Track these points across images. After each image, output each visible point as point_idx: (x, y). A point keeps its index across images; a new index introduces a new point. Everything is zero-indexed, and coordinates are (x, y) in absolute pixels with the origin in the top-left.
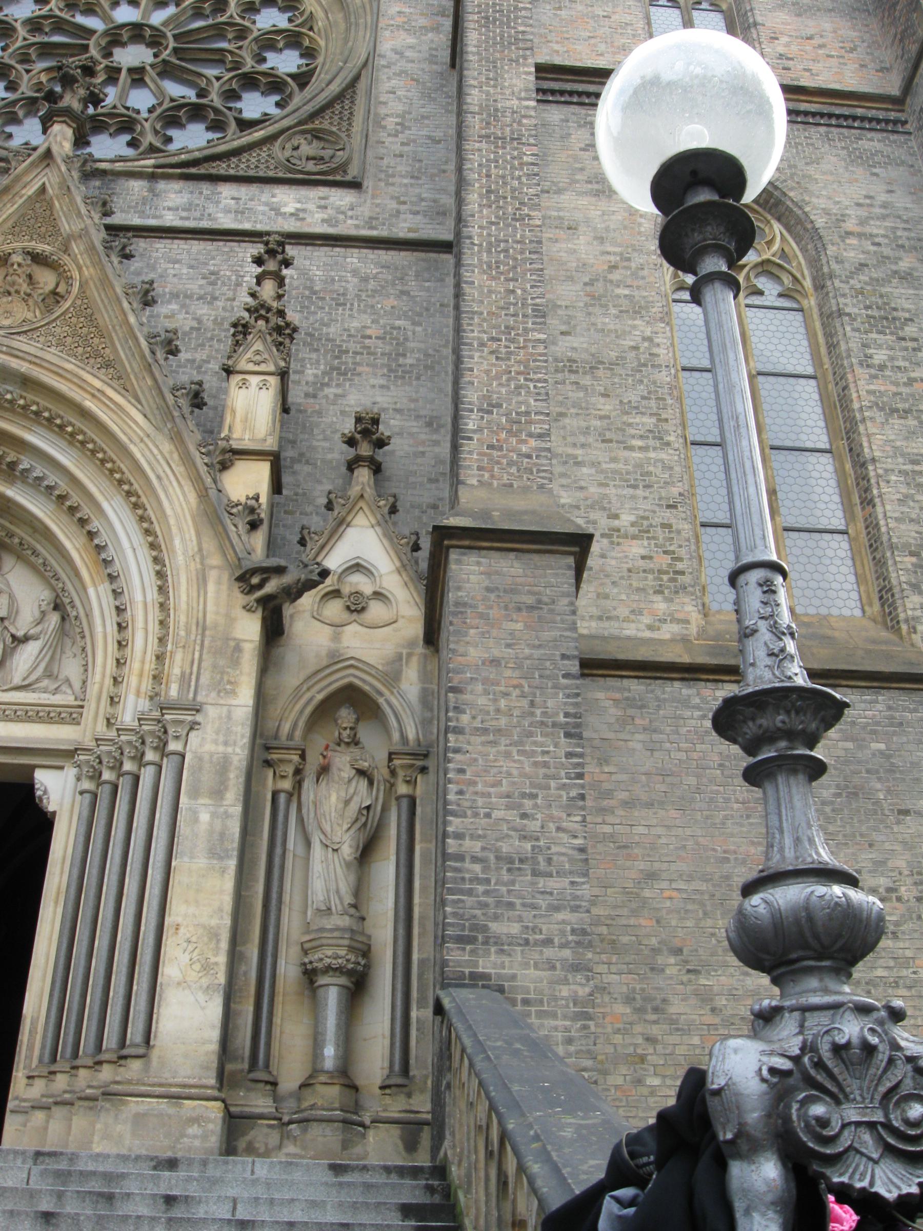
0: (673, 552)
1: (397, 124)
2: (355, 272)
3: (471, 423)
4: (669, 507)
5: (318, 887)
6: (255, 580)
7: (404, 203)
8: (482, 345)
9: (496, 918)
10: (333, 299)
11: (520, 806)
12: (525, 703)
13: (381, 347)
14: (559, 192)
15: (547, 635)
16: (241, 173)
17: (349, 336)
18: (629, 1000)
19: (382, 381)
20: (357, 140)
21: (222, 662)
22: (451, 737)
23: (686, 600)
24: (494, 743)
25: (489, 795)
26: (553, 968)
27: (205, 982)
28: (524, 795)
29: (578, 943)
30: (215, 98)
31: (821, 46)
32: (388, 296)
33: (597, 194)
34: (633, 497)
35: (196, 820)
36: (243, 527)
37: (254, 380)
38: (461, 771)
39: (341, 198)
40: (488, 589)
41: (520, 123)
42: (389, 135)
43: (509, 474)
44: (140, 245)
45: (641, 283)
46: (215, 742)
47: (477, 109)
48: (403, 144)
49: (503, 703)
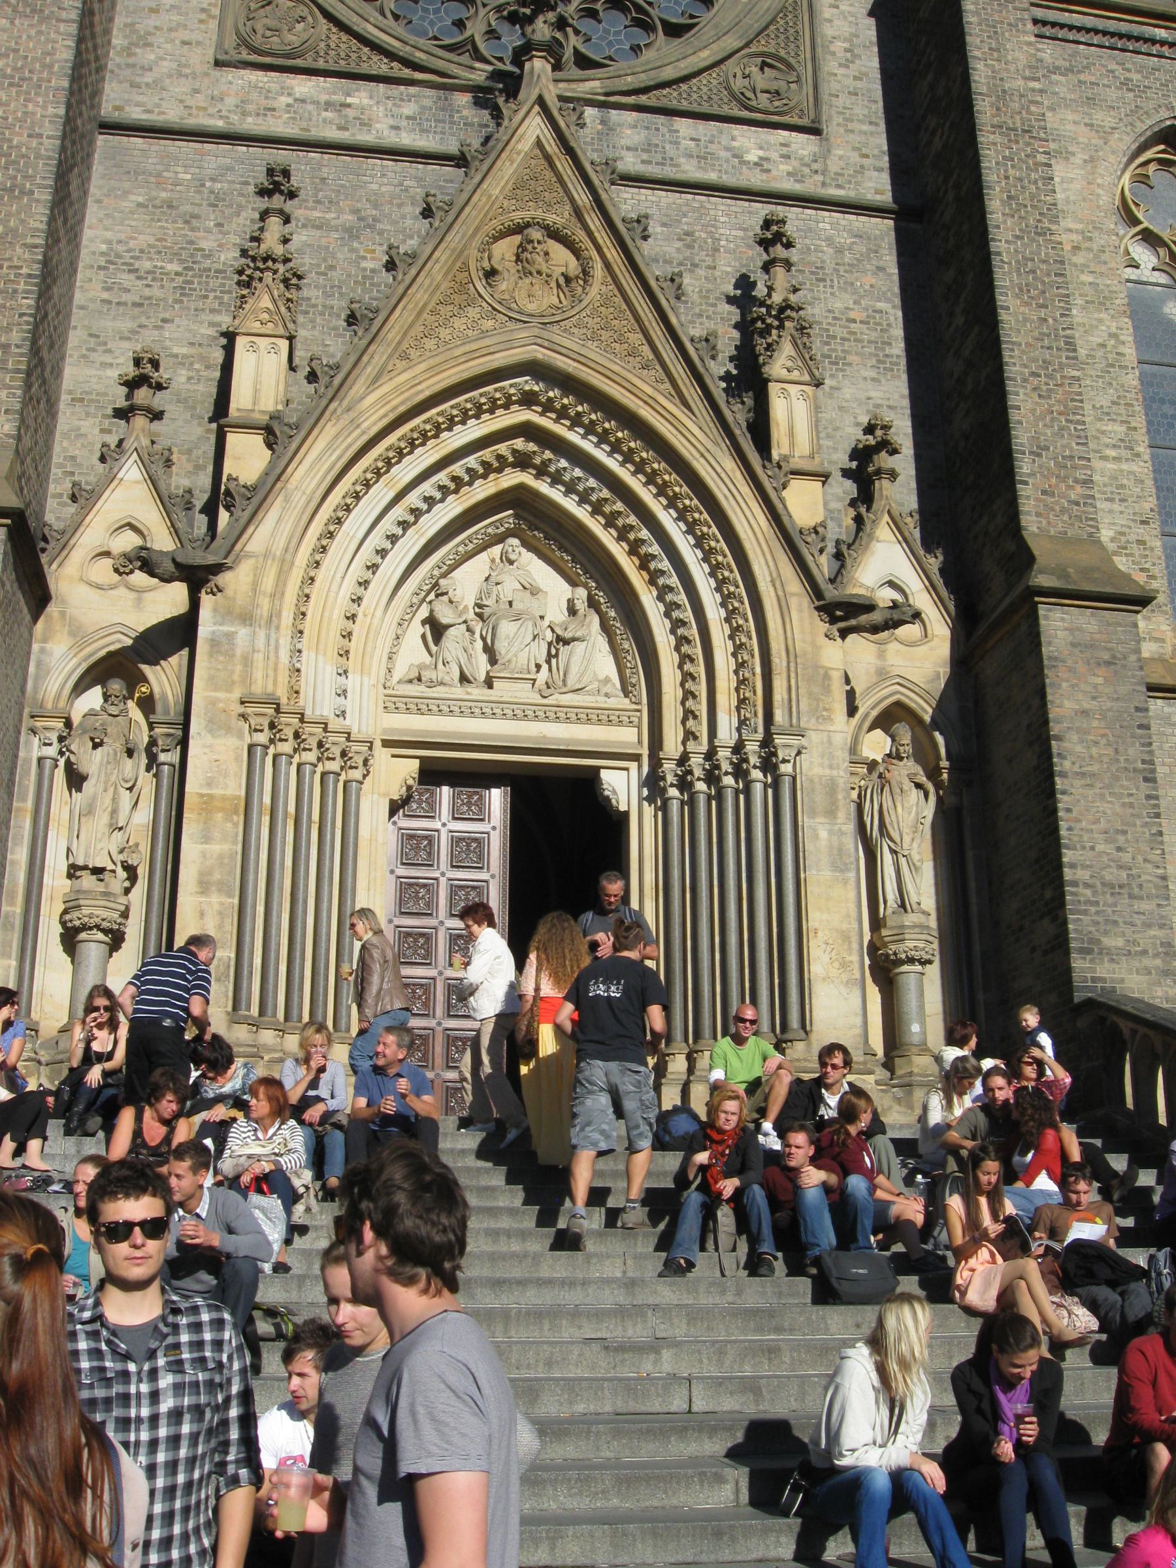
0: (1148, 570)
1: (847, 50)
2: (829, 240)
3: (1024, 466)
4: (1143, 522)
6: (839, 613)
7: (867, 156)
8: (1025, 380)
9: (1106, 933)
10: (812, 273)
11: (1115, 841)
12: (1110, 751)
13: (868, 335)
15: (1123, 689)
16: (695, 108)
17: (835, 318)
21: (816, 690)
22: (1058, 780)
23: (1161, 619)
24: (1091, 786)
25: (1092, 831)
26: (1150, 973)
27: (845, 977)
28: (1117, 832)
29: (1166, 954)
32: (864, 272)
34: (1111, 511)
35: (816, 837)
36: (816, 554)
37: (793, 389)
38: (1069, 810)
39: (802, 144)
40: (1073, 645)
41: (1029, 112)
42: (840, 65)
43: (1064, 522)
45: (1103, 268)
46: (822, 765)
47: (984, 90)
48: (855, 78)
49: (1094, 751)
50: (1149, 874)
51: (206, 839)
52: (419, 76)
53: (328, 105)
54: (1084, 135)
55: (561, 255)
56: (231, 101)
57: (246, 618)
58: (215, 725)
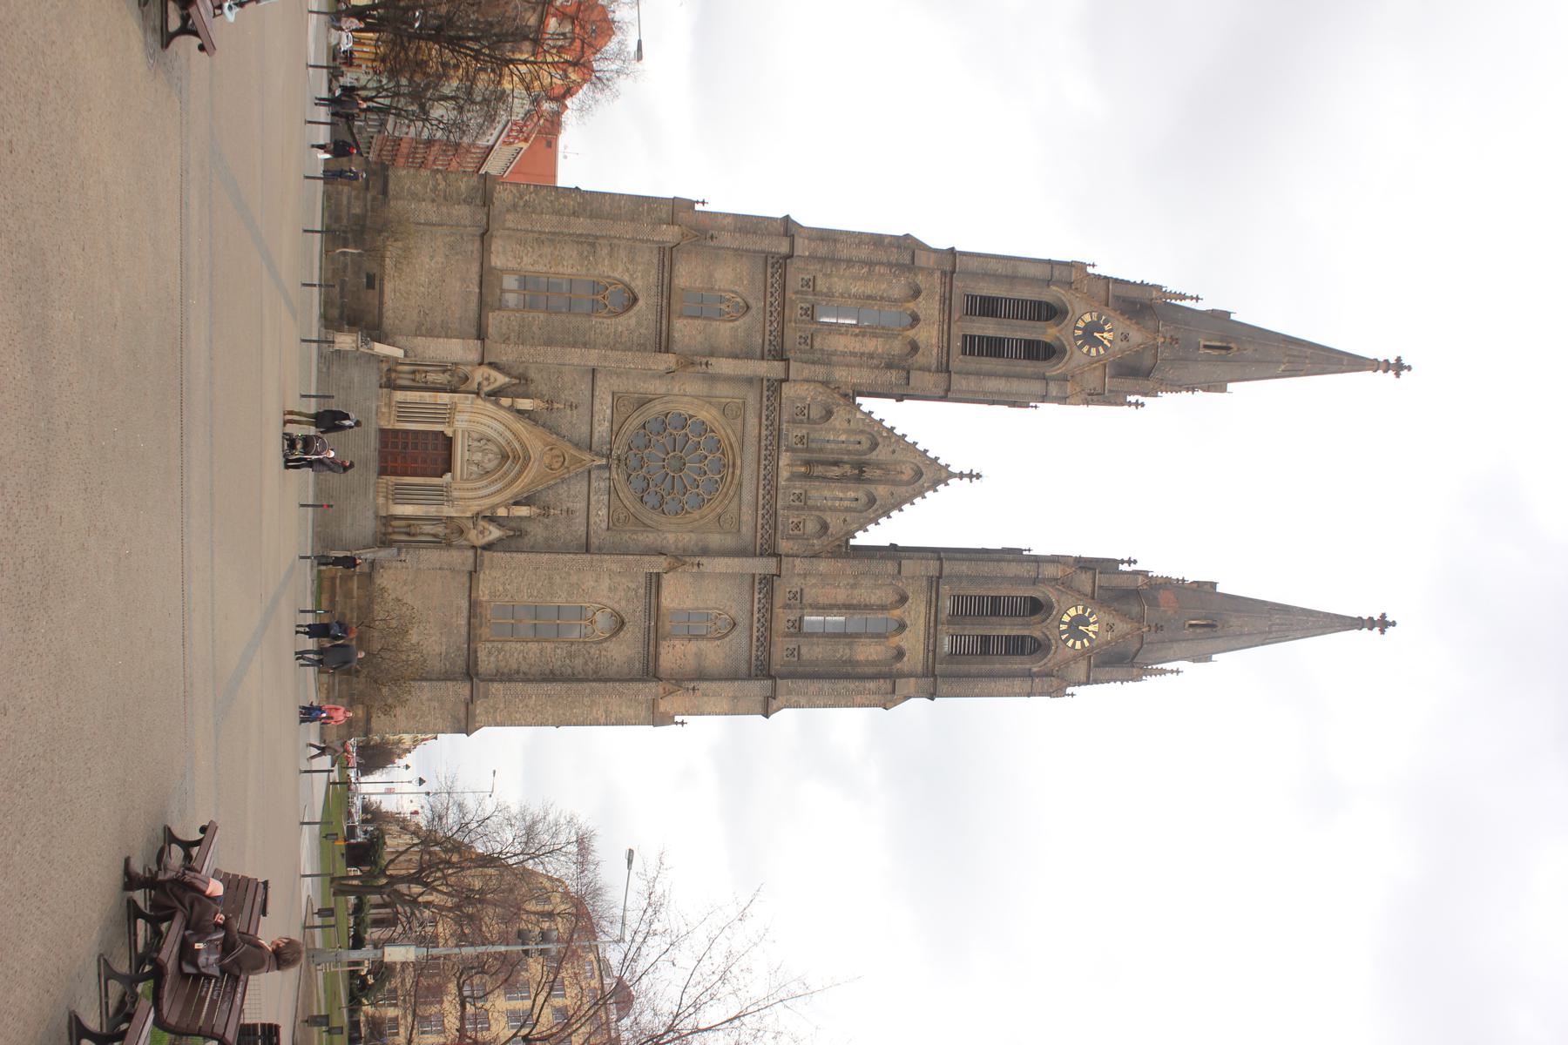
5: (424, 527)
20: (627, 528)
30: (652, 489)
31: (681, 659)
33: (610, 588)
39: (604, 525)
44: (587, 479)
52: (613, 438)
55: (559, 464)
56: (604, 396)
57: (472, 403)
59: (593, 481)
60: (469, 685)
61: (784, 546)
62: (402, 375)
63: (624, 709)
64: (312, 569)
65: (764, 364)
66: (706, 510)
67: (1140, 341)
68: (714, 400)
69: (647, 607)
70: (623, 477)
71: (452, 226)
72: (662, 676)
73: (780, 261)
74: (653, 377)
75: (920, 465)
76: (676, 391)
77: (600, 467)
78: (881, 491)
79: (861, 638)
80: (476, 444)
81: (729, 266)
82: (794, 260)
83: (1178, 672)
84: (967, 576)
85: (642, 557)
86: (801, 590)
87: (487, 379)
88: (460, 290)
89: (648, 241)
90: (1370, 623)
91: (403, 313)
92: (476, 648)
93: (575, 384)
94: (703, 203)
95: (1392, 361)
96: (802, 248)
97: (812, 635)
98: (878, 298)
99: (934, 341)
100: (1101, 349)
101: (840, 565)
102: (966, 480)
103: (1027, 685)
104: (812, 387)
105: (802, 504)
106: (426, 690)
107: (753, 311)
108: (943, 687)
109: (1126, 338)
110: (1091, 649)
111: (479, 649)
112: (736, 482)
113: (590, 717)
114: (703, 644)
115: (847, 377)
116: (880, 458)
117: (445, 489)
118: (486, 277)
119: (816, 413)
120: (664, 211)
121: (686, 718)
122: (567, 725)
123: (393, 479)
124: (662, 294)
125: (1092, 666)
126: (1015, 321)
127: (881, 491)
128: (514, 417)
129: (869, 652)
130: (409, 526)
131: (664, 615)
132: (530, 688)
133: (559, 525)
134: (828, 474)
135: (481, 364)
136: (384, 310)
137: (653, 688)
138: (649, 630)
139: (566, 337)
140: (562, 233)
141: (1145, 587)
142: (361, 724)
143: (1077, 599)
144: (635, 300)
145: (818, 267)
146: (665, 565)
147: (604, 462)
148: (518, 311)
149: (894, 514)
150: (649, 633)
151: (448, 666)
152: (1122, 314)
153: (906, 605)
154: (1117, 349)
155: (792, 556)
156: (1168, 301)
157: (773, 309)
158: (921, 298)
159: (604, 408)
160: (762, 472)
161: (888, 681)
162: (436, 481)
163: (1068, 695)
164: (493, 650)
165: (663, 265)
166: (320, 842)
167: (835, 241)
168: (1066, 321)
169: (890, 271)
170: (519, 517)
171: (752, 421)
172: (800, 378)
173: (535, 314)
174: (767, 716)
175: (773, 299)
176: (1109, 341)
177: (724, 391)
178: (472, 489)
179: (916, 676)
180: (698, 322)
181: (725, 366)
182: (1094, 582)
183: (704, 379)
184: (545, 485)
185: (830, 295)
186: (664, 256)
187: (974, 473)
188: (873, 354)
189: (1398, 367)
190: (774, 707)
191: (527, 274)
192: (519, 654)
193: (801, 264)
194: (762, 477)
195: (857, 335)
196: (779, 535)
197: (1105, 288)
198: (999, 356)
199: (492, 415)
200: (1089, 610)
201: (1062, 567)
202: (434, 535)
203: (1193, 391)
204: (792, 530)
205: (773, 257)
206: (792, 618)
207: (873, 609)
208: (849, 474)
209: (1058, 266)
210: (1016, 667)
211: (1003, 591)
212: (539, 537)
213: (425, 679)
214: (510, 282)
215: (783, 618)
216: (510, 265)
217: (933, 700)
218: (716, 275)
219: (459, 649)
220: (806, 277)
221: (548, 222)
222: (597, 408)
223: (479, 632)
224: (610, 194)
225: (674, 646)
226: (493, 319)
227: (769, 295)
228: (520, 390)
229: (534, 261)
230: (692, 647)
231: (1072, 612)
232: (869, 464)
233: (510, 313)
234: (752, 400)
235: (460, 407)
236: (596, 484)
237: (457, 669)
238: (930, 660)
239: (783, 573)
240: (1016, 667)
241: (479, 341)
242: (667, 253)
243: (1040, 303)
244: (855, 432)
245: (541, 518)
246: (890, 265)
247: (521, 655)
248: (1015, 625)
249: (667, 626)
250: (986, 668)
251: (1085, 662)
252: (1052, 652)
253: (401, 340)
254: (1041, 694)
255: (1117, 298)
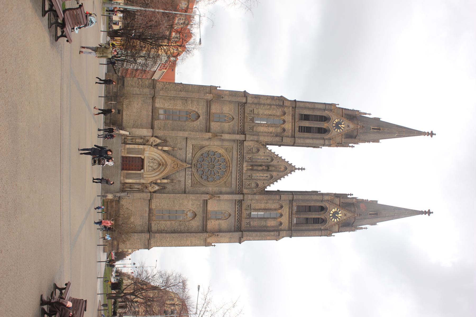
14: (192, 202)
18: (130, 202)
19: (172, 188)
30: (205, 174)
31: (214, 226)
33: (192, 204)
39: (190, 185)
44: (185, 171)
50: (134, 198)
51: (137, 146)
52: (193, 158)
53: (190, 152)
54: (194, 207)
55: (176, 167)
56: (190, 146)
57: (150, 148)
58: (143, 147)
59: (186, 172)
60: (149, 234)
61: (245, 191)
62: (128, 140)
63: (196, 241)
64: (101, 199)
65: (238, 135)
66: (221, 180)
67: (353, 127)
68: (223, 147)
69: (203, 210)
70: (196, 171)
71: (144, 95)
72: (208, 231)
73: (243, 104)
74: (205, 140)
75: (286, 166)
76: (212, 144)
77: (189, 167)
78: (274, 174)
79: (269, 219)
80: (151, 161)
81: (227, 106)
82: (247, 104)
83: (366, 228)
84: (301, 200)
85: (202, 195)
86: (250, 204)
87: (154, 141)
88: (146, 114)
89: (203, 99)
90: (425, 213)
91: (129, 121)
92: (151, 223)
93: (181, 142)
94: (220, 87)
95: (430, 132)
96: (250, 100)
97: (254, 218)
98: (273, 115)
99: (290, 128)
100: (341, 130)
101: (262, 197)
102: (300, 170)
103: (320, 233)
104: (253, 143)
105: (250, 178)
106: (136, 236)
107: (235, 120)
108: (294, 234)
109: (348, 126)
110: (339, 222)
111: (152, 223)
112: (230, 171)
113: (186, 244)
114: (220, 221)
115: (264, 139)
116: (274, 164)
117: (141, 175)
118: (154, 110)
119: (254, 150)
120: (207, 90)
121: (215, 244)
122: (179, 246)
123: (126, 172)
124: (207, 115)
125: (340, 227)
126: (315, 122)
127: (274, 174)
128: (163, 153)
129: (271, 223)
130: (131, 186)
131: (208, 213)
132: (168, 235)
133: (176, 185)
134: (258, 169)
135: (152, 136)
136: (123, 121)
137: (205, 235)
138: (204, 217)
139: (178, 128)
140: (177, 97)
141: (356, 202)
142: (116, 247)
143: (335, 206)
144: (199, 117)
145: (255, 106)
146: (209, 197)
147: (190, 166)
148: (163, 120)
149: (279, 181)
150: (204, 218)
151: (142, 229)
152: (347, 119)
153: (282, 209)
154: (346, 130)
155: (247, 194)
156: (361, 115)
157: (241, 119)
158: (286, 115)
159: (190, 149)
160: (238, 169)
161: (277, 232)
162: (139, 172)
163: (333, 236)
164: (156, 223)
165: (208, 106)
166: (103, 283)
167: (260, 98)
168: (330, 122)
169: (277, 107)
170: (164, 183)
171: (235, 153)
172: (249, 140)
173: (169, 121)
174: (240, 243)
175: (241, 116)
176: (343, 128)
177: (226, 144)
178: (150, 174)
179: (286, 231)
180: (219, 123)
181: (226, 136)
182: (340, 201)
183: (220, 140)
184: (172, 173)
185: (258, 114)
186: (208, 103)
187: (303, 168)
188: (271, 132)
189: (432, 134)
190: (242, 240)
191: (166, 109)
192: (164, 225)
193: (249, 105)
194: (238, 170)
195: (266, 127)
196: (243, 188)
197: (342, 111)
198: (310, 133)
199: (155, 152)
200: (339, 210)
201: (330, 197)
202: (138, 189)
203: (369, 142)
204: (248, 186)
205: (241, 103)
206: (248, 213)
207: (272, 210)
208: (264, 169)
209: (327, 105)
210: (316, 227)
211: (312, 204)
212: (170, 189)
213: (135, 233)
214: (161, 112)
215: (245, 213)
216: (161, 107)
217: (291, 238)
218: (224, 109)
219: (146, 223)
220: (251, 109)
221: (173, 93)
222: (188, 149)
223: (152, 218)
224: (191, 85)
225: (212, 222)
226: (156, 123)
227: (240, 115)
228: (164, 144)
229: (168, 105)
230: (217, 222)
231: (334, 210)
232: (271, 166)
233: (161, 121)
234: (235, 146)
235: (146, 149)
236: (188, 173)
237: (145, 229)
238: (290, 226)
239: (245, 199)
240: (316, 227)
241: (152, 130)
242: (209, 102)
243: (322, 116)
244: (266, 156)
245: (171, 183)
246: (276, 105)
247: (165, 225)
248: (316, 215)
249: (209, 216)
250: (307, 228)
251: (338, 226)
252: (328, 222)
253: (128, 129)
254: (324, 236)
255: (346, 114)
